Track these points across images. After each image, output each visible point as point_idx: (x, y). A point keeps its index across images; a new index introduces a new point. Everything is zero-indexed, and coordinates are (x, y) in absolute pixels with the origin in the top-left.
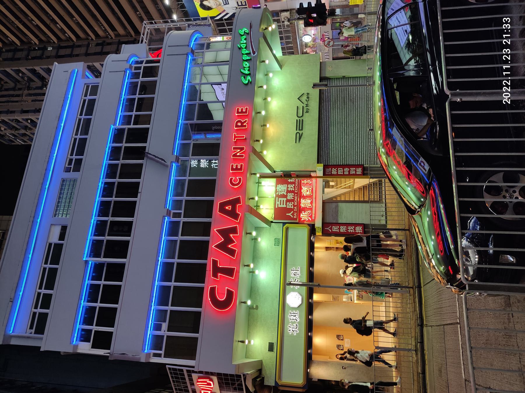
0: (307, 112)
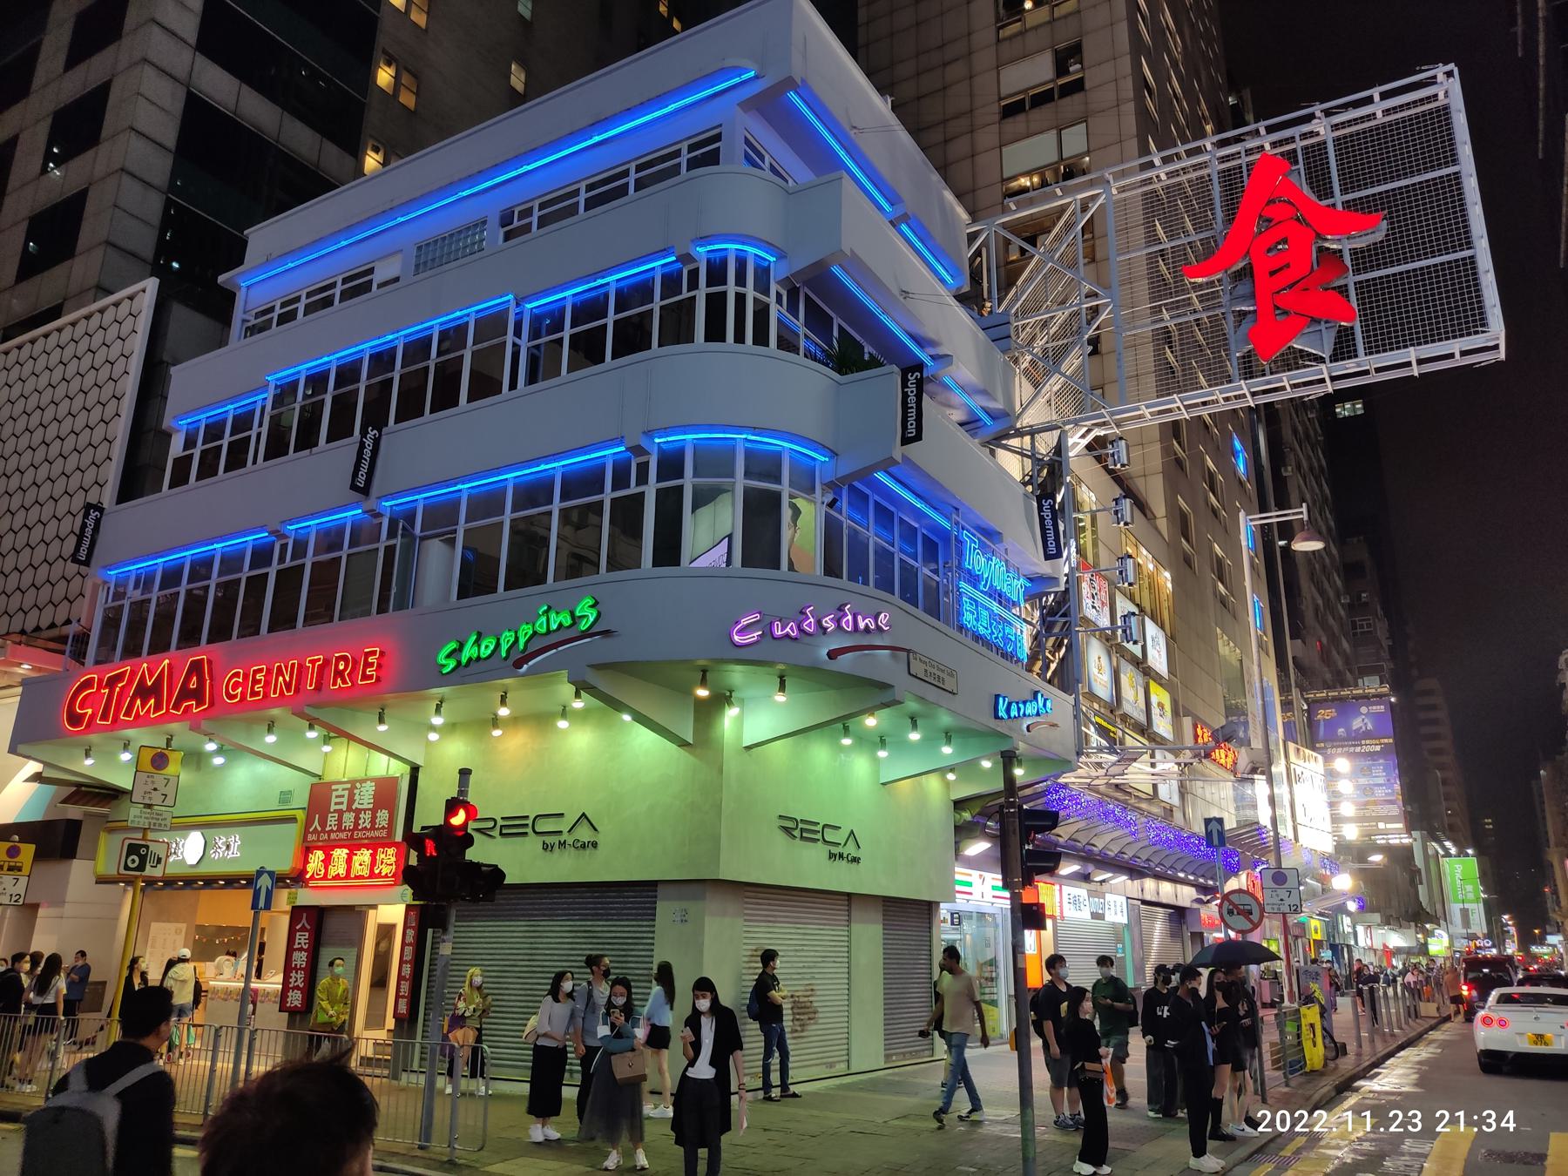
0: (546, 847)
